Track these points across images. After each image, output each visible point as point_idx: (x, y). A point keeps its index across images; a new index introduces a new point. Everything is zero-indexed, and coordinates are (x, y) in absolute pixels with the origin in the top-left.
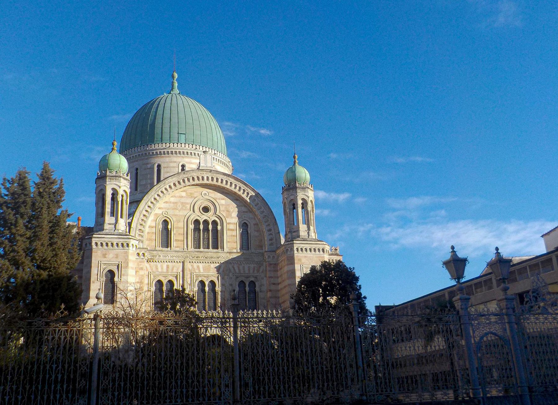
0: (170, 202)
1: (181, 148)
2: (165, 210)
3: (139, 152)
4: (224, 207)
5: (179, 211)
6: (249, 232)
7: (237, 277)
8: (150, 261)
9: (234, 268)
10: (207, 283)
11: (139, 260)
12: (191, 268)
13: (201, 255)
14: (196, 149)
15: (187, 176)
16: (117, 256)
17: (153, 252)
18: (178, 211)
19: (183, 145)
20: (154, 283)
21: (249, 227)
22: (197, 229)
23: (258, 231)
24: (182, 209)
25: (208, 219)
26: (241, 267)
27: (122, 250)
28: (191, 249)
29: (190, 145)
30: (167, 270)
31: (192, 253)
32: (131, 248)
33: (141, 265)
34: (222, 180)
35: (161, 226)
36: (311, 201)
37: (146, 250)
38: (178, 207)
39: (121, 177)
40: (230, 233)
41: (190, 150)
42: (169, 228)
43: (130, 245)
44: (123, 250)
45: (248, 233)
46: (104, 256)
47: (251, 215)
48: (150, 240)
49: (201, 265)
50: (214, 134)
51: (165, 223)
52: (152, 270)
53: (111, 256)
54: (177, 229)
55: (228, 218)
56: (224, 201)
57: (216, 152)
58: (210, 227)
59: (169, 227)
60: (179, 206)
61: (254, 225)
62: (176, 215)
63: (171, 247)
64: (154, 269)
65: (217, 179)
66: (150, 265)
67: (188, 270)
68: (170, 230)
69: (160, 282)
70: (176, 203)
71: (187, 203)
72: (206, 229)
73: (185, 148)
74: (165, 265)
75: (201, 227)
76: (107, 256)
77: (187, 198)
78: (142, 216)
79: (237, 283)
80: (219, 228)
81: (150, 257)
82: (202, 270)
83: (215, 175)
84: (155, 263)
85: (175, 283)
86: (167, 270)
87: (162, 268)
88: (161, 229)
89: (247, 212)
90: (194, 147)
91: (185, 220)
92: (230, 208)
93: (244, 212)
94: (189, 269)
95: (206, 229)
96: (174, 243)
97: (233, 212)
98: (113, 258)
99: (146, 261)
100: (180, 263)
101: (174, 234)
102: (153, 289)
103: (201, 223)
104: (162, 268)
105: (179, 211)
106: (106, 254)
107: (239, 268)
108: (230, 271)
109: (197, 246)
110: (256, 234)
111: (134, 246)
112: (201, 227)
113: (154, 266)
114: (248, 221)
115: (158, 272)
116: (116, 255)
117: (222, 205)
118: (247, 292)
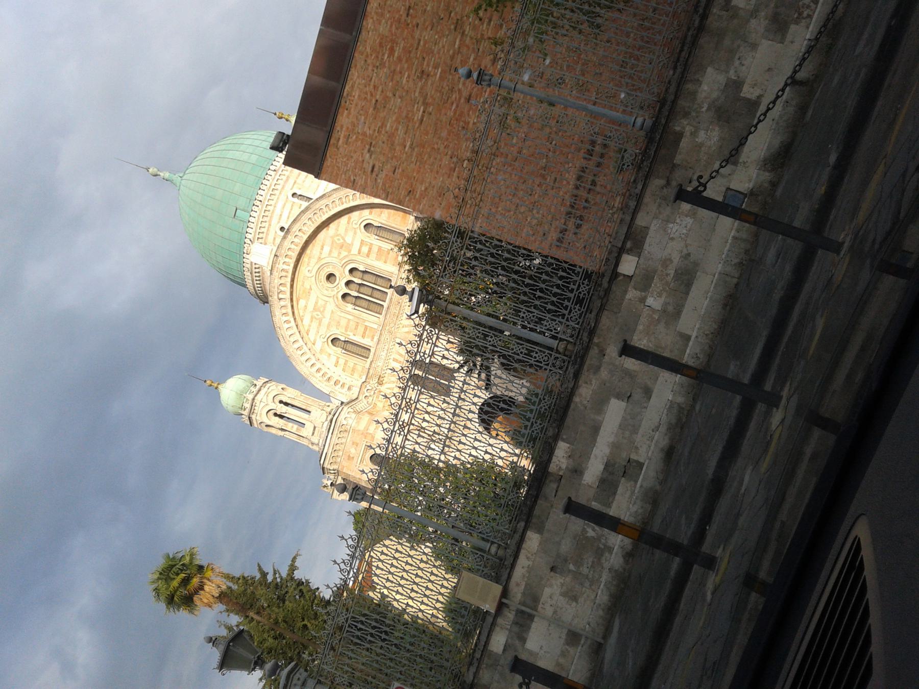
0: (310, 326)
1: (255, 224)
4: (334, 250)
5: (324, 317)
6: (380, 225)
8: (382, 381)
11: (375, 399)
14: (261, 201)
16: (355, 444)
18: (324, 320)
19: (252, 219)
27: (350, 436)
28: (381, 319)
29: (254, 209)
31: (386, 321)
32: (350, 421)
35: (339, 350)
37: (363, 386)
39: (253, 399)
40: (373, 255)
41: (260, 212)
43: (345, 422)
46: (350, 458)
48: (353, 370)
50: (245, 157)
51: (334, 341)
53: (353, 451)
54: (349, 330)
55: (350, 251)
56: (325, 247)
57: (272, 168)
59: (343, 339)
60: (318, 315)
62: (329, 325)
63: (370, 347)
70: (312, 318)
71: (316, 303)
73: (257, 218)
76: (351, 456)
77: (308, 300)
80: (362, 268)
83: (283, 251)
88: (343, 351)
89: (350, 218)
90: (258, 203)
91: (339, 313)
93: (348, 223)
94: (406, 332)
96: (366, 342)
99: (380, 387)
105: (324, 317)
106: (349, 456)
111: (348, 416)
113: (390, 378)
116: (353, 444)
117: (331, 251)
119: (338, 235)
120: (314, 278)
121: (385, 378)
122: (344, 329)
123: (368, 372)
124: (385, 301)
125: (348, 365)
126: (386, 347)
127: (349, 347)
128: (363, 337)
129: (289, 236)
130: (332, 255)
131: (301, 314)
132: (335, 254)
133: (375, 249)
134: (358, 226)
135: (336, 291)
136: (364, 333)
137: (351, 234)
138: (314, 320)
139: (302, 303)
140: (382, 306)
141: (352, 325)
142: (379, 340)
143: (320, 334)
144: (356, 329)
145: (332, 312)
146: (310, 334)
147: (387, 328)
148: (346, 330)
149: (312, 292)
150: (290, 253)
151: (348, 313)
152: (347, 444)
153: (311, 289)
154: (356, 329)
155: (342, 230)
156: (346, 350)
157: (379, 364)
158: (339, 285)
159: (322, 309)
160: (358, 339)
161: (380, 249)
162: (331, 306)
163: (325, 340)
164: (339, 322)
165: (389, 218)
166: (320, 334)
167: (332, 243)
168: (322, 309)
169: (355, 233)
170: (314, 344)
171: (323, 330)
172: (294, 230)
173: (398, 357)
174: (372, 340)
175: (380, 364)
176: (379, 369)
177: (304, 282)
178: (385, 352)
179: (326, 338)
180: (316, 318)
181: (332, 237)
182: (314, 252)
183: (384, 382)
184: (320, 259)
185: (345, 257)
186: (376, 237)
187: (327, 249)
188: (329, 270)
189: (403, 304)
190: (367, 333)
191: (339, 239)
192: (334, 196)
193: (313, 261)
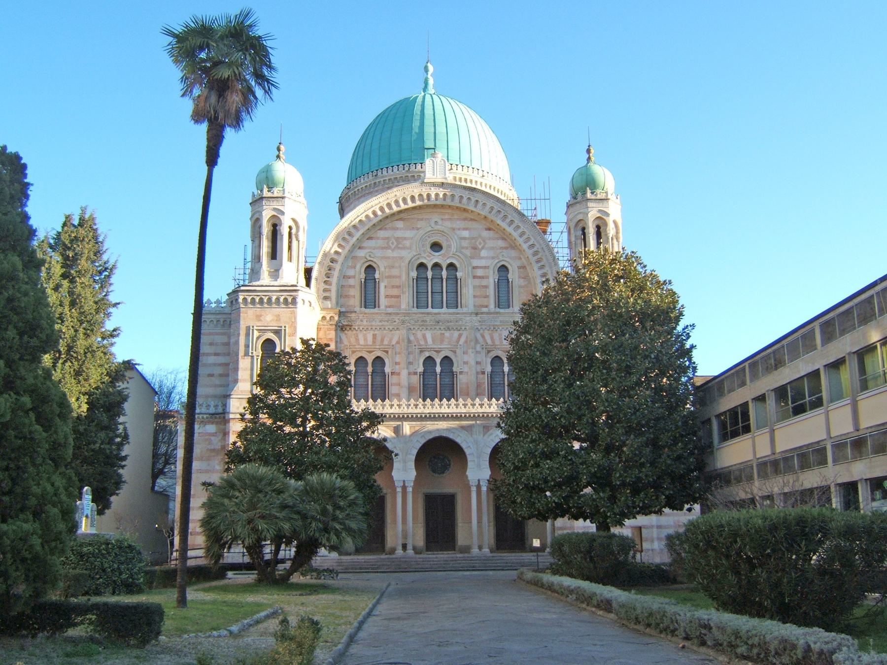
3: (364, 183)
4: (467, 241)
6: (510, 280)
7: (489, 352)
9: (483, 336)
10: (438, 361)
12: (412, 338)
13: (428, 318)
18: (390, 251)
21: (510, 271)
22: (421, 279)
23: (526, 277)
24: (397, 247)
26: (496, 336)
31: (414, 315)
33: (329, 334)
34: (461, 197)
35: (363, 276)
36: (615, 222)
40: (477, 282)
45: (508, 282)
47: (513, 253)
51: (370, 269)
52: (349, 342)
55: (472, 257)
58: (444, 273)
59: (377, 276)
61: (519, 268)
63: (379, 307)
64: (353, 340)
67: (406, 341)
68: (377, 280)
70: (388, 238)
71: (405, 239)
72: (437, 278)
75: (430, 274)
79: (489, 360)
80: (459, 274)
85: (387, 361)
86: (374, 342)
87: (365, 339)
88: (363, 280)
89: (506, 248)
92: (478, 243)
93: (501, 248)
95: (437, 278)
96: (383, 301)
97: (483, 248)
101: (385, 287)
103: (429, 267)
104: (365, 339)
107: (492, 338)
108: (477, 341)
109: (420, 303)
110: (522, 282)
112: (430, 274)
114: (509, 263)
117: (465, 238)
118: (506, 373)
119: (484, 241)
120: (430, 229)
121: (350, 332)
122: (387, 274)
124: (432, 308)
128: (387, 296)
129: (467, 192)
130: (463, 241)
131: (387, 226)
132: (465, 244)
133: (484, 282)
134: (501, 258)
135: (425, 256)
136: (392, 297)
137: (491, 254)
139: (400, 224)
141: (396, 282)
142: (390, 314)
143: (373, 251)
144: (393, 287)
145: (401, 258)
146: (370, 241)
148: (389, 277)
149: (414, 232)
153: (418, 229)
154: (393, 287)
155: (490, 244)
156: (365, 282)
158: (433, 257)
159: (400, 246)
161: (486, 287)
162: (407, 255)
163: (369, 259)
164: (393, 267)
165: (520, 287)
166: (373, 251)
167: (473, 238)
168: (400, 246)
169: (493, 258)
170: (360, 248)
171: (379, 253)
172: (475, 194)
173: (379, 338)
174: (386, 307)
177: (422, 220)
178: (381, 324)
179: (372, 259)
180: (388, 242)
182: (458, 222)
183: (346, 332)
184: (454, 229)
185: (466, 256)
186: (496, 280)
187: (466, 234)
189: (438, 327)
191: (480, 243)
193: (448, 224)
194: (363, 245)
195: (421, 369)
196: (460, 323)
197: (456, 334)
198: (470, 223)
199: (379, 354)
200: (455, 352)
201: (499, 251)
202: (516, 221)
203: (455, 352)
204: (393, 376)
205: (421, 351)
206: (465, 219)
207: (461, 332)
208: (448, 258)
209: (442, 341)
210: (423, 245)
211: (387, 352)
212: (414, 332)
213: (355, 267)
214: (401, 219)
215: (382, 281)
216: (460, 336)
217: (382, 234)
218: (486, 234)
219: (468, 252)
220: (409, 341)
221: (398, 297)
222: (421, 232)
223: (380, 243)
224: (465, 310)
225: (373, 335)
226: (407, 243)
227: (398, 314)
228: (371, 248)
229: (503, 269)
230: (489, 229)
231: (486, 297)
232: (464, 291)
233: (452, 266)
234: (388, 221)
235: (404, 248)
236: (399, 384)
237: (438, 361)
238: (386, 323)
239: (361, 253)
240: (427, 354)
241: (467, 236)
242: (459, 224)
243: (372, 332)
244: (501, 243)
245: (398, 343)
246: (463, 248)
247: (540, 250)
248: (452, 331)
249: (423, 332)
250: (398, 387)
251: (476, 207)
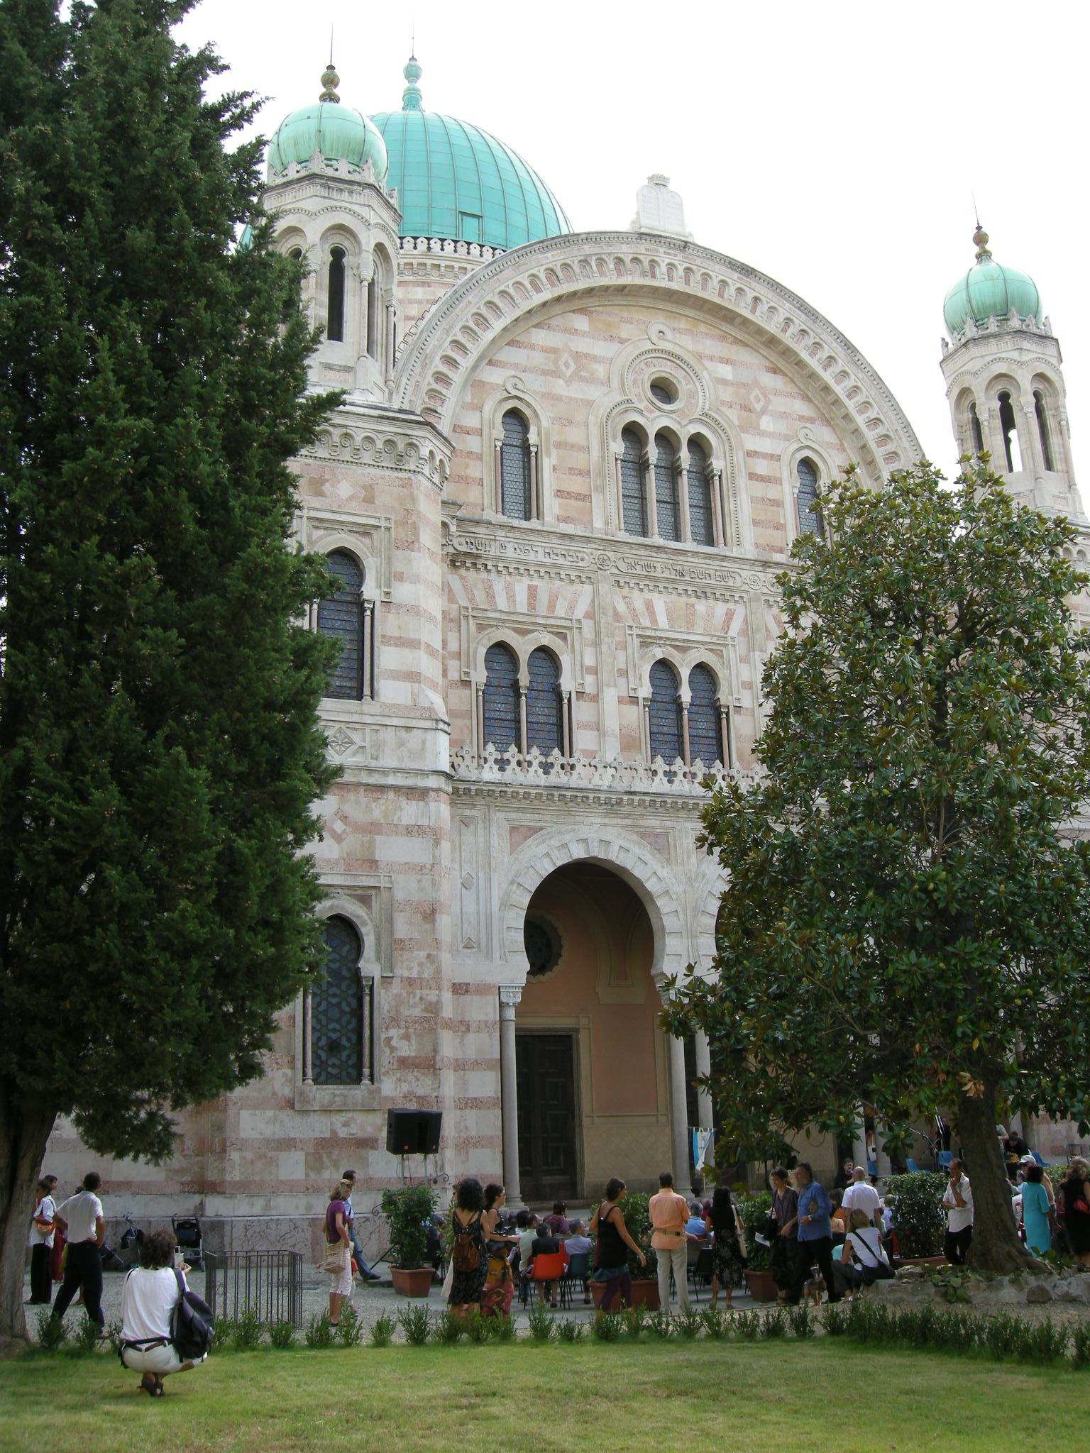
0: (532, 347)
2: (513, 373)
4: (730, 389)
5: (568, 382)
10: (685, 673)
12: (621, 607)
13: (659, 560)
15: (597, 250)
17: (476, 530)
18: (561, 382)
20: (482, 652)
24: (576, 376)
25: (674, 427)
27: (388, 473)
30: (529, 604)
34: (723, 283)
35: (499, 432)
38: (564, 368)
40: (759, 489)
42: (531, 442)
44: (400, 475)
49: (659, 602)
51: (516, 418)
52: (472, 600)
55: (744, 428)
59: (533, 438)
60: (567, 365)
65: (706, 276)
66: (462, 578)
68: (533, 449)
69: (502, 650)
70: (554, 351)
71: (595, 358)
74: (521, 586)
76: (327, 488)
78: (429, 378)
81: (463, 548)
82: (663, 621)
83: (698, 262)
84: (484, 575)
85: (565, 660)
86: (532, 606)
88: (499, 444)
89: (812, 420)
92: (752, 398)
93: (802, 418)
94: (615, 610)
96: (551, 505)
97: (764, 411)
98: (350, 499)
100: (577, 586)
101: (554, 469)
102: (480, 675)
104: (511, 598)
105: (568, 382)
113: (481, 586)
114: (821, 456)
115: (495, 611)
116: (364, 487)
117: (724, 382)
119: (765, 396)
120: (650, 346)
121: (472, 573)
122: (555, 437)
123: (478, 523)
125: (472, 463)
126: (560, 561)
127: (515, 455)
128: (559, 493)
129: (736, 275)
131: (553, 322)
132: (726, 394)
135: (641, 406)
136: (569, 495)
137: (781, 427)
138: (552, 356)
139: (581, 322)
140: (644, 533)
141: (578, 460)
142: (570, 537)
145: (589, 404)
147: (611, 554)
148: (559, 445)
149: (615, 346)
150: (697, 277)
151: (604, 445)
152: (360, 470)
153: (622, 341)
155: (778, 404)
157: (510, 547)
158: (658, 413)
159: (583, 374)
160: (549, 481)
163: (515, 392)
164: (570, 422)
167: (744, 385)
170: (490, 363)
172: (754, 284)
173: (543, 598)
175: (510, 553)
176: (494, 551)
178: (547, 560)
180: (556, 362)
181: (756, 383)
182: (708, 342)
183: (462, 571)
184: (700, 357)
188: (683, 383)
189: (680, 587)
190: (572, 502)
192: (861, 376)
193: (687, 341)
194: (495, 358)
195: (645, 691)
196: (731, 583)
197: (721, 609)
198: (734, 348)
199: (546, 639)
200: (720, 654)
201: (798, 423)
202: (840, 361)
203: (720, 654)
204: (581, 703)
205: (646, 642)
206: (722, 338)
207: (731, 605)
208: (691, 421)
209: (690, 623)
210: (635, 382)
211: (563, 637)
212: (626, 591)
213: (480, 409)
214: (582, 311)
215: (549, 456)
216: (729, 616)
217: (541, 337)
218: (769, 380)
219: (733, 415)
220: (617, 616)
221: (586, 498)
222: (630, 351)
223: (538, 358)
224: (735, 552)
225: (530, 587)
226: (601, 370)
227: (588, 540)
228: (516, 366)
229: (808, 467)
230: (775, 370)
231: (779, 527)
232: (730, 506)
233: (697, 443)
234: (557, 309)
235: (592, 380)
236: (598, 727)
237: (685, 673)
238: (560, 561)
239: (494, 376)
240: (659, 653)
241: (730, 377)
242: (710, 346)
243: (526, 581)
244: (800, 407)
245: (590, 615)
246: (723, 403)
247: (891, 434)
248: (711, 602)
249: (647, 595)
250: (595, 733)
251: (753, 311)
